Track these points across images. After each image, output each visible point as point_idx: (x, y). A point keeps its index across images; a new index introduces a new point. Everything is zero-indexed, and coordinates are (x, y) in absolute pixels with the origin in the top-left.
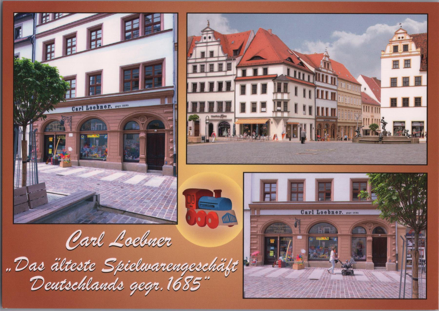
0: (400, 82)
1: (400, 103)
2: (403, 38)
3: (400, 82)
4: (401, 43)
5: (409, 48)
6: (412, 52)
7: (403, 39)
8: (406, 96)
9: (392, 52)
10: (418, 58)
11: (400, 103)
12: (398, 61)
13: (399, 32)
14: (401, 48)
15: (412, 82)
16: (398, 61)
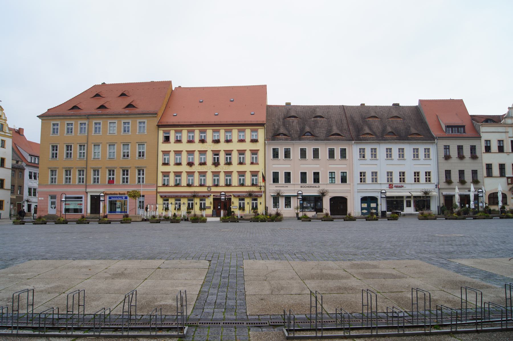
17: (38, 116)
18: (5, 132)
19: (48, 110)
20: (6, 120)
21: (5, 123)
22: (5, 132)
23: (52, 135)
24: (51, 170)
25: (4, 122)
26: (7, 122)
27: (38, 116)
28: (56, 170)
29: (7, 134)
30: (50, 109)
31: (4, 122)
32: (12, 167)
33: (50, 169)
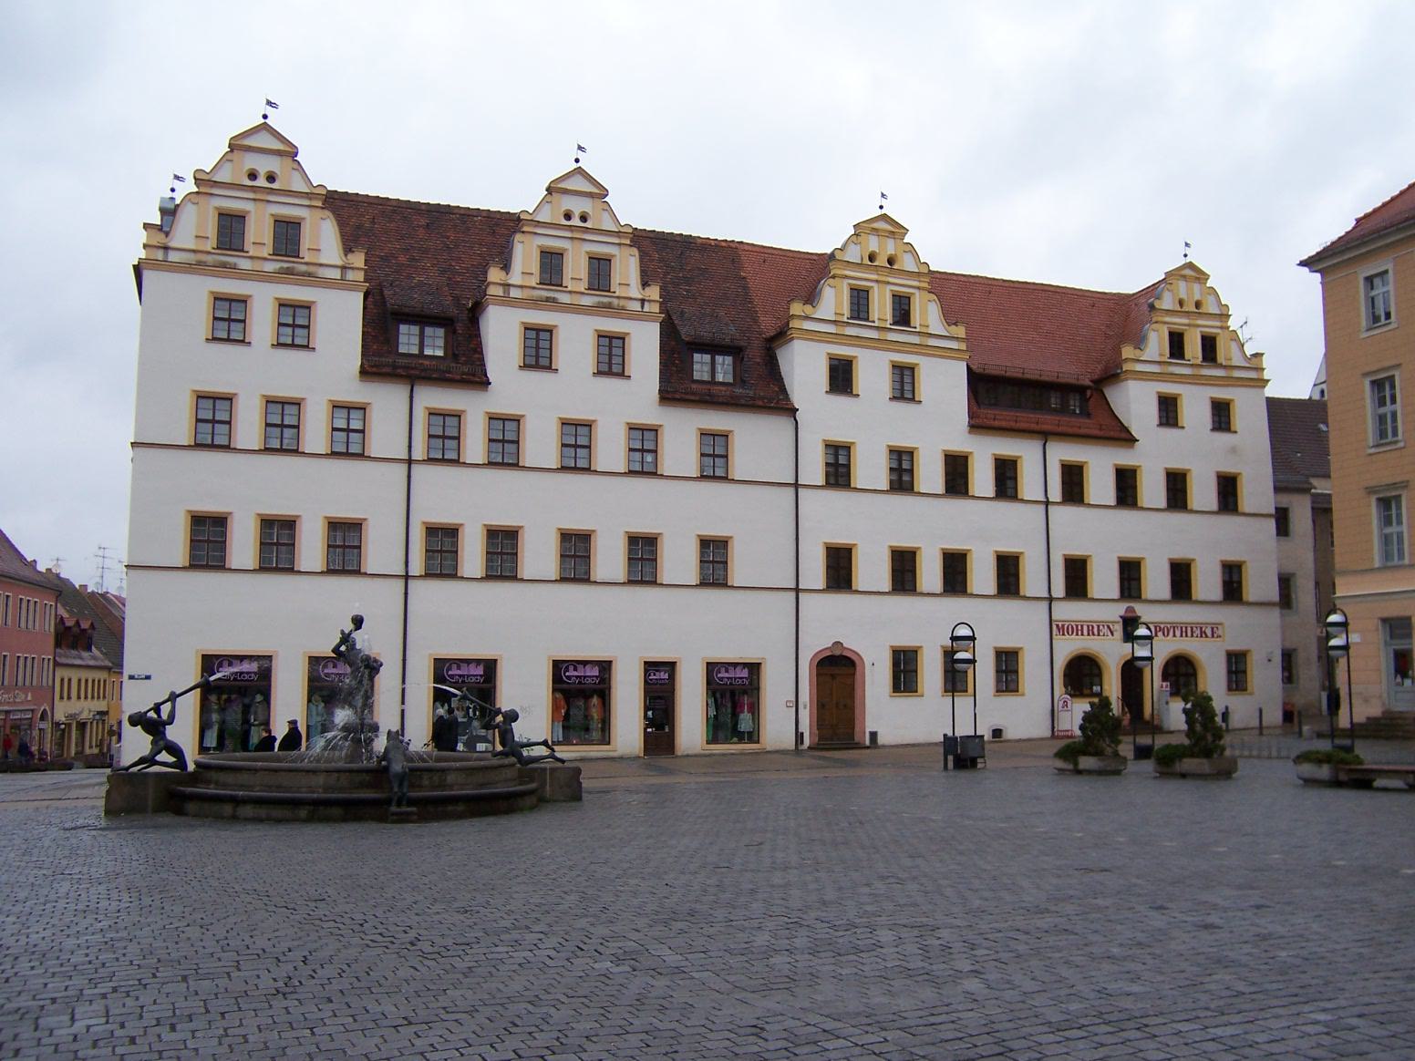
0: (248, 428)
1: (243, 545)
2: (271, 178)
3: (248, 428)
4: (261, 205)
5: (306, 243)
6: (321, 265)
7: (274, 186)
8: (279, 508)
9: (210, 245)
10: (353, 305)
11: (243, 545)
12: (243, 301)
13: (252, 142)
14: (259, 232)
15: (316, 434)
16: (243, 301)
17: (1303, 264)
18: (1225, 367)
19: (1358, 220)
20: (1224, 316)
21: (1221, 328)
22: (1225, 367)
23: (1369, 329)
24: (1379, 500)
25: (1218, 324)
26: (1233, 324)
27: (1303, 264)
28: (1400, 496)
29: (1237, 374)
30: (1367, 216)
31: (1218, 324)
32: (1276, 508)
33: (1375, 492)
